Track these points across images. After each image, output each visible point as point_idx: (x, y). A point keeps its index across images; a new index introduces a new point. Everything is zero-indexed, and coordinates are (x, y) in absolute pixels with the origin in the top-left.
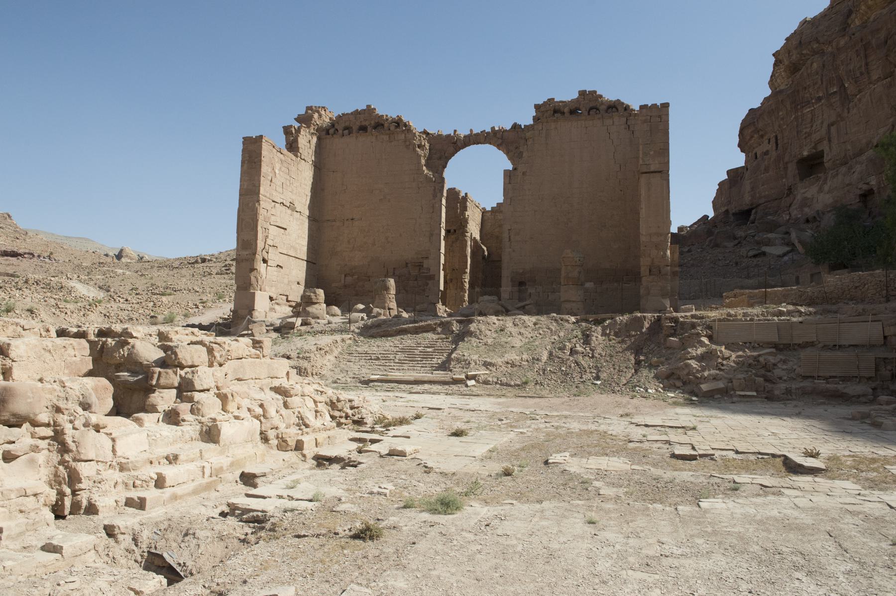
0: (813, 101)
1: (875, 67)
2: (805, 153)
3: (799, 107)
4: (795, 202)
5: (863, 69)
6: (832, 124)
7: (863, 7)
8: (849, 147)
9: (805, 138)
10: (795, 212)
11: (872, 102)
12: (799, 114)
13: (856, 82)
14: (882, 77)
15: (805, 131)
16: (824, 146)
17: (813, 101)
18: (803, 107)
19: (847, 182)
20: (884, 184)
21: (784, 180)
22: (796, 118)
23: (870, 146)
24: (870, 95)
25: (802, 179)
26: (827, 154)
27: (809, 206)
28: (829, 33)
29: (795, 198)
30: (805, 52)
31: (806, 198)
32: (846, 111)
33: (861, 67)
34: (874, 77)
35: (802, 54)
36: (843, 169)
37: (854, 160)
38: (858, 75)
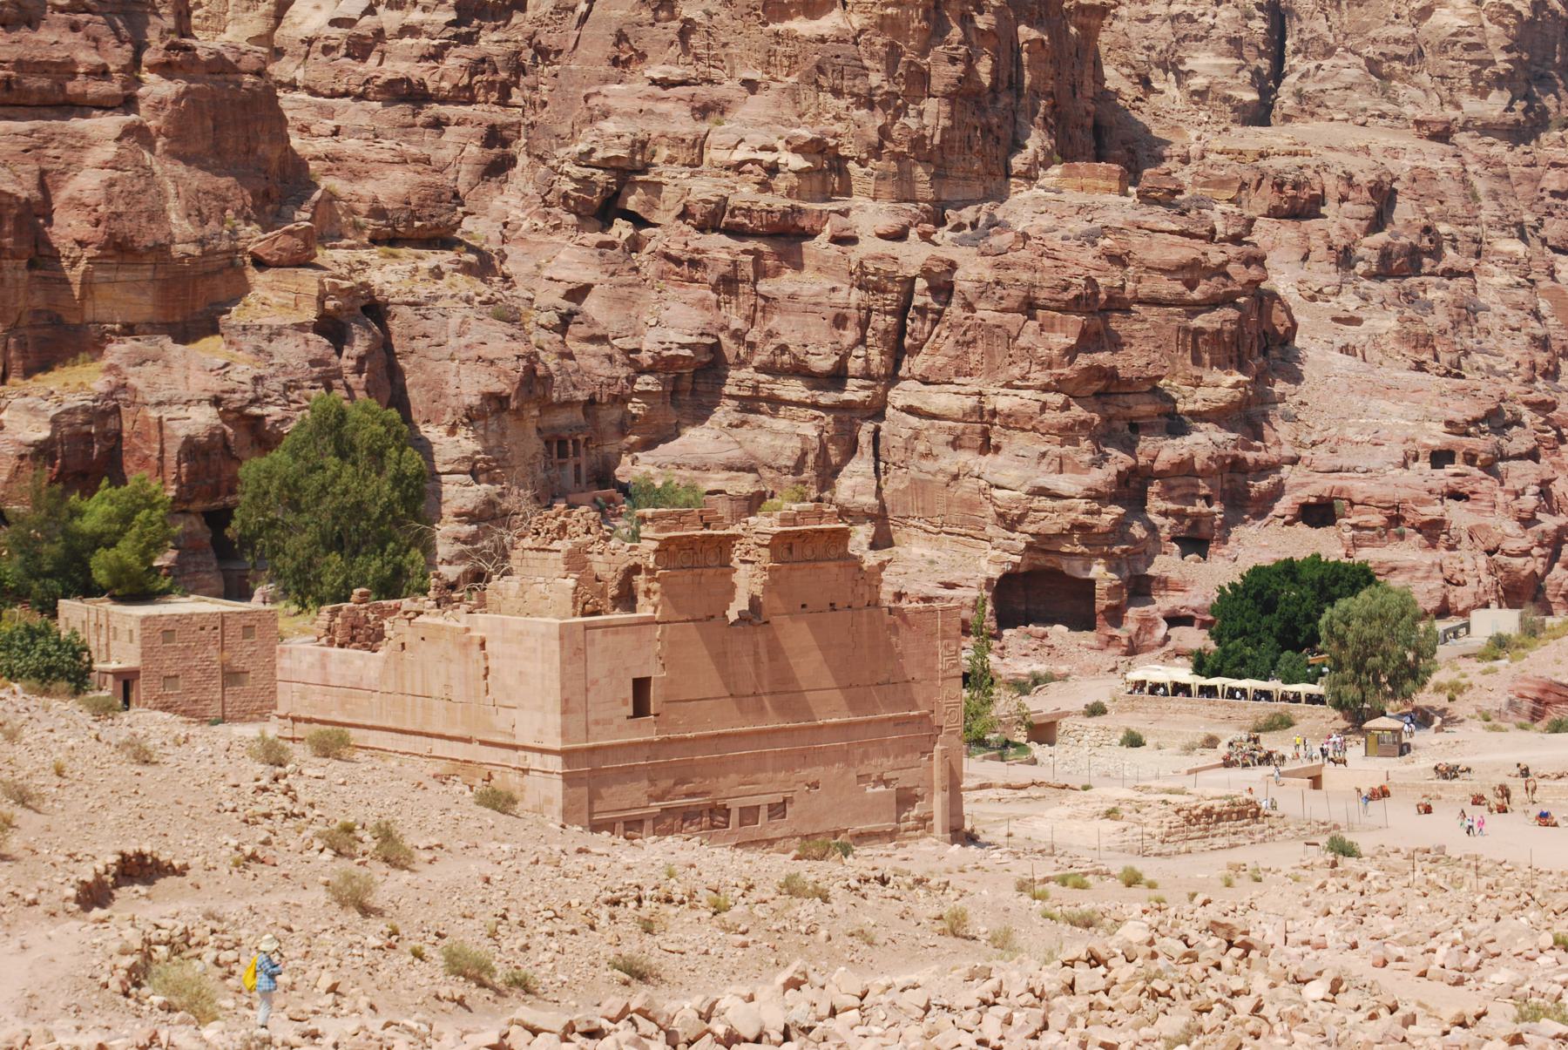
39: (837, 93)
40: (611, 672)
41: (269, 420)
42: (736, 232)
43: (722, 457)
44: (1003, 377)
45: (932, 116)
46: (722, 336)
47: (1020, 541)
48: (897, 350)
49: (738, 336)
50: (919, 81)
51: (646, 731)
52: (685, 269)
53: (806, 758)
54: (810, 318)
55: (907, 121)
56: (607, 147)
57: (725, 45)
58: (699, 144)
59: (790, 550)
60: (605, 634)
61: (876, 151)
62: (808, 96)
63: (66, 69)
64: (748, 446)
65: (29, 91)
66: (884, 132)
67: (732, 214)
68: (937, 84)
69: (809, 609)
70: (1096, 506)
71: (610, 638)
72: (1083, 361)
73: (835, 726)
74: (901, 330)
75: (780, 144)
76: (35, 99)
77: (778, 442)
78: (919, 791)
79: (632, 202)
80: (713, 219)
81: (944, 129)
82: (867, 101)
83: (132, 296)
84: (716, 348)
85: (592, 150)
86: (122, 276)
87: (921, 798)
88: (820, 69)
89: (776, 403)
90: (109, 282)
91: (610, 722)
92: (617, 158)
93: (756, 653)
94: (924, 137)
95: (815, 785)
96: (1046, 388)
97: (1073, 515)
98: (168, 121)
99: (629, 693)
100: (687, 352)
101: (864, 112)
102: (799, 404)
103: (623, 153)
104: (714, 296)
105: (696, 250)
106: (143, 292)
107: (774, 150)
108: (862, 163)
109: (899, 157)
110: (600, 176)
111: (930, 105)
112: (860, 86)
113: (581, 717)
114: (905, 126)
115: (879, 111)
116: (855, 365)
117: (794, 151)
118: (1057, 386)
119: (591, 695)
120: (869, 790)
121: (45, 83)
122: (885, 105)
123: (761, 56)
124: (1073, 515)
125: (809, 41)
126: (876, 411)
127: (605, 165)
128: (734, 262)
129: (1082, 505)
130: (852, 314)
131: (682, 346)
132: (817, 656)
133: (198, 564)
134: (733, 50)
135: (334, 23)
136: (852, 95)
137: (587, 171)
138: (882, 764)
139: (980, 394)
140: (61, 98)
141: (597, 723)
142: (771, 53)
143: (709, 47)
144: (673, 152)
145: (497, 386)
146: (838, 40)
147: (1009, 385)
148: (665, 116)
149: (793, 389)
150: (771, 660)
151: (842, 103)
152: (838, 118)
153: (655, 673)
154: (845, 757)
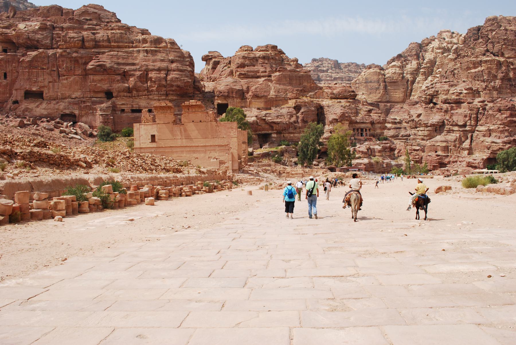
0: (39, 68)
1: (77, 70)
2: (34, 89)
3: (31, 68)
4: (19, 108)
5: (73, 68)
6: (50, 82)
7: (72, 44)
8: (59, 94)
9: (34, 82)
10: (19, 113)
11: (74, 82)
12: (31, 71)
13: (68, 71)
14: (80, 75)
15: (34, 79)
16: (45, 91)
17: (39, 68)
18: (33, 68)
19: (57, 108)
20: (82, 114)
21: (8, 95)
22: (29, 72)
23: (69, 97)
24: (74, 79)
25: (25, 99)
26: (46, 94)
27: (29, 112)
28: (45, 42)
29: (19, 106)
30: (29, 42)
31: (28, 108)
32: (58, 80)
33: (71, 67)
34: (77, 73)
35: (27, 42)
36: (54, 102)
37: (61, 100)
38: (70, 69)
39: (478, 80)
40: (146, 133)
41: (266, 120)
42: (449, 103)
43: (440, 140)
44: (493, 123)
45: (498, 83)
46: (445, 120)
47: (490, 152)
48: (477, 120)
49: (447, 120)
50: (495, 77)
51: (154, 145)
52: (440, 110)
53: (194, 152)
54: (460, 116)
55: (491, 84)
56: (429, 92)
57: (460, 76)
58: (448, 91)
59: (189, 110)
60: (144, 126)
61: (485, 89)
62: (473, 82)
63: (258, 72)
64: (447, 138)
65: (249, 75)
66: (486, 86)
67: (448, 100)
68: (499, 77)
69: (194, 122)
70: (504, 144)
71: (146, 127)
72: (509, 119)
73: (201, 146)
74: (477, 117)
75: (463, 89)
76: (251, 76)
77: (452, 137)
78: (226, 161)
79: (434, 101)
80: (445, 102)
81: (500, 85)
82: (483, 81)
83: (259, 104)
84: (443, 122)
85: (427, 93)
86: (257, 101)
87: (226, 163)
88: (475, 77)
89: (453, 131)
90: (255, 101)
91: (146, 143)
92: (431, 94)
93: (181, 130)
94: (495, 86)
95: (197, 158)
96: (501, 124)
97: (499, 146)
98: (276, 78)
99: (150, 137)
100: (437, 123)
101: (483, 83)
102: (457, 131)
103: (432, 93)
104: (444, 114)
105: (442, 107)
106: (262, 103)
107: (462, 90)
108: (482, 92)
109: (489, 90)
110: (428, 97)
111: (497, 81)
112: (482, 79)
113: (139, 142)
114: (491, 85)
115: (486, 83)
116: (468, 124)
117: (466, 90)
118: (503, 124)
119: (141, 138)
120: (212, 160)
121: (253, 74)
122: (487, 81)
123: (466, 77)
124: (499, 146)
125: (473, 73)
126: (473, 131)
127: (429, 95)
128: (447, 108)
129: (501, 144)
130: (468, 115)
131: (436, 122)
132: (196, 132)
133: (254, 142)
134: (461, 76)
135: (426, 87)
136: (480, 80)
137: (426, 96)
138: (216, 155)
139: (489, 127)
140: (256, 76)
141: (143, 143)
142: (468, 76)
143: (457, 76)
144: (443, 92)
145: (335, 117)
146: (478, 72)
147: (493, 124)
148: (444, 87)
149: (456, 128)
150: (185, 132)
151: (479, 82)
152: (478, 85)
153: (155, 133)
154: (205, 152)
